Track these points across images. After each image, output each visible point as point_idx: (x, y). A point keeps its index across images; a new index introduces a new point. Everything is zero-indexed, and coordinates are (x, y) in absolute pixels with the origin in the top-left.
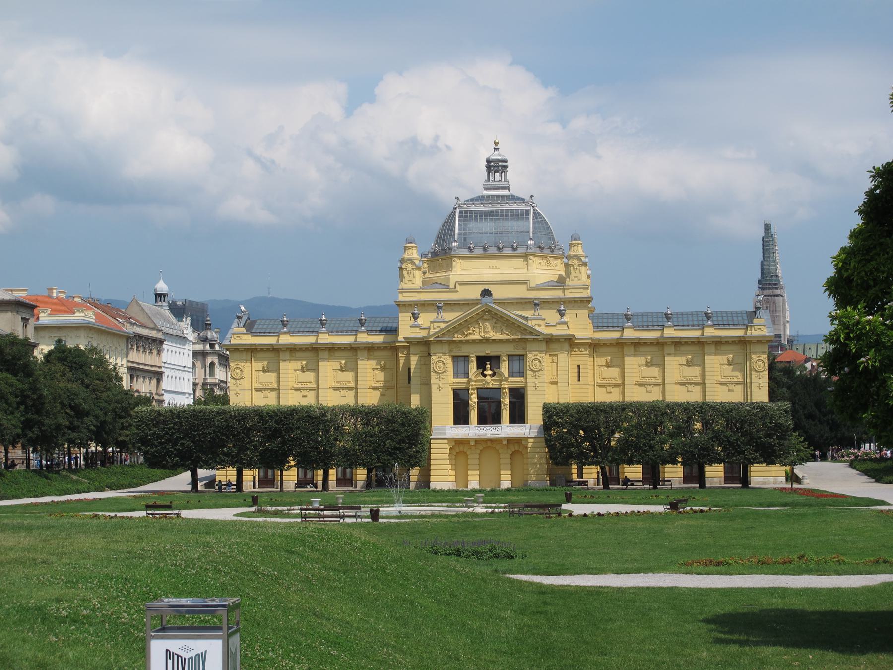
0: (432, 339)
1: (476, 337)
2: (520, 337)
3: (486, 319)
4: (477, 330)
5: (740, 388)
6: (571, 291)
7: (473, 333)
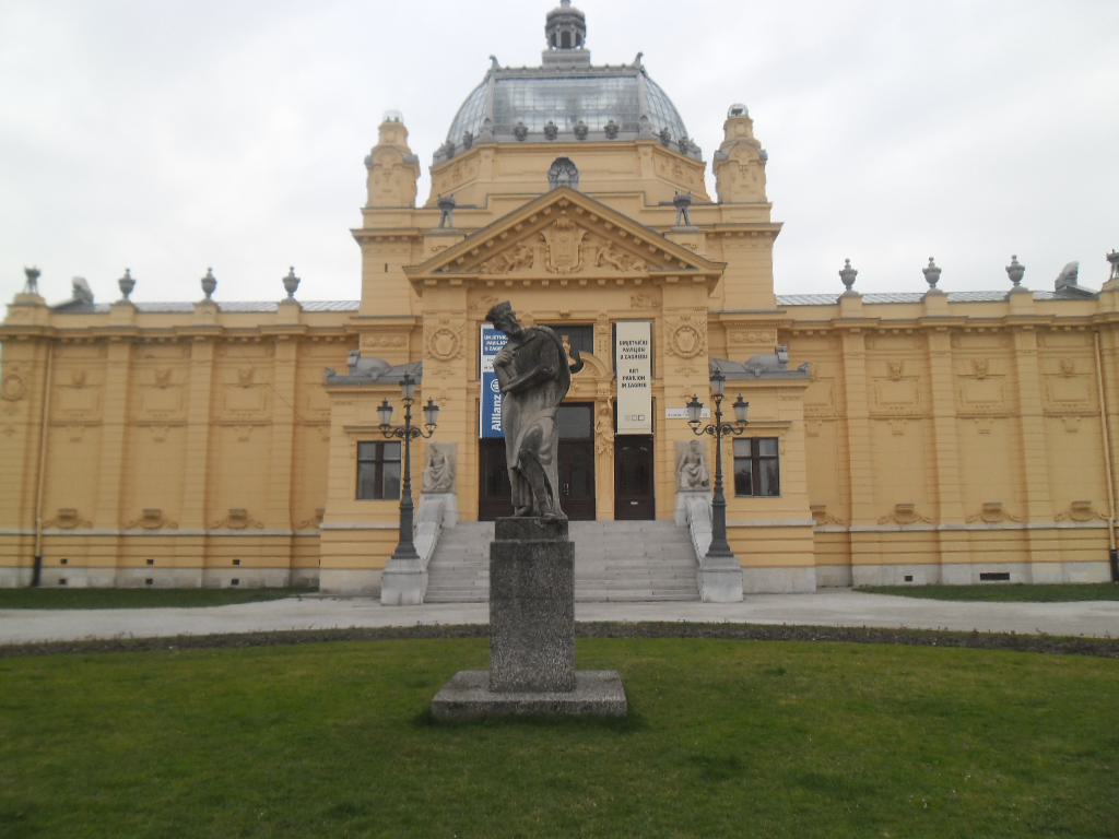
0: (426, 274)
1: (537, 272)
2: (644, 274)
3: (561, 228)
4: (537, 255)
5: (1088, 426)
6: (735, 214)
7: (528, 262)
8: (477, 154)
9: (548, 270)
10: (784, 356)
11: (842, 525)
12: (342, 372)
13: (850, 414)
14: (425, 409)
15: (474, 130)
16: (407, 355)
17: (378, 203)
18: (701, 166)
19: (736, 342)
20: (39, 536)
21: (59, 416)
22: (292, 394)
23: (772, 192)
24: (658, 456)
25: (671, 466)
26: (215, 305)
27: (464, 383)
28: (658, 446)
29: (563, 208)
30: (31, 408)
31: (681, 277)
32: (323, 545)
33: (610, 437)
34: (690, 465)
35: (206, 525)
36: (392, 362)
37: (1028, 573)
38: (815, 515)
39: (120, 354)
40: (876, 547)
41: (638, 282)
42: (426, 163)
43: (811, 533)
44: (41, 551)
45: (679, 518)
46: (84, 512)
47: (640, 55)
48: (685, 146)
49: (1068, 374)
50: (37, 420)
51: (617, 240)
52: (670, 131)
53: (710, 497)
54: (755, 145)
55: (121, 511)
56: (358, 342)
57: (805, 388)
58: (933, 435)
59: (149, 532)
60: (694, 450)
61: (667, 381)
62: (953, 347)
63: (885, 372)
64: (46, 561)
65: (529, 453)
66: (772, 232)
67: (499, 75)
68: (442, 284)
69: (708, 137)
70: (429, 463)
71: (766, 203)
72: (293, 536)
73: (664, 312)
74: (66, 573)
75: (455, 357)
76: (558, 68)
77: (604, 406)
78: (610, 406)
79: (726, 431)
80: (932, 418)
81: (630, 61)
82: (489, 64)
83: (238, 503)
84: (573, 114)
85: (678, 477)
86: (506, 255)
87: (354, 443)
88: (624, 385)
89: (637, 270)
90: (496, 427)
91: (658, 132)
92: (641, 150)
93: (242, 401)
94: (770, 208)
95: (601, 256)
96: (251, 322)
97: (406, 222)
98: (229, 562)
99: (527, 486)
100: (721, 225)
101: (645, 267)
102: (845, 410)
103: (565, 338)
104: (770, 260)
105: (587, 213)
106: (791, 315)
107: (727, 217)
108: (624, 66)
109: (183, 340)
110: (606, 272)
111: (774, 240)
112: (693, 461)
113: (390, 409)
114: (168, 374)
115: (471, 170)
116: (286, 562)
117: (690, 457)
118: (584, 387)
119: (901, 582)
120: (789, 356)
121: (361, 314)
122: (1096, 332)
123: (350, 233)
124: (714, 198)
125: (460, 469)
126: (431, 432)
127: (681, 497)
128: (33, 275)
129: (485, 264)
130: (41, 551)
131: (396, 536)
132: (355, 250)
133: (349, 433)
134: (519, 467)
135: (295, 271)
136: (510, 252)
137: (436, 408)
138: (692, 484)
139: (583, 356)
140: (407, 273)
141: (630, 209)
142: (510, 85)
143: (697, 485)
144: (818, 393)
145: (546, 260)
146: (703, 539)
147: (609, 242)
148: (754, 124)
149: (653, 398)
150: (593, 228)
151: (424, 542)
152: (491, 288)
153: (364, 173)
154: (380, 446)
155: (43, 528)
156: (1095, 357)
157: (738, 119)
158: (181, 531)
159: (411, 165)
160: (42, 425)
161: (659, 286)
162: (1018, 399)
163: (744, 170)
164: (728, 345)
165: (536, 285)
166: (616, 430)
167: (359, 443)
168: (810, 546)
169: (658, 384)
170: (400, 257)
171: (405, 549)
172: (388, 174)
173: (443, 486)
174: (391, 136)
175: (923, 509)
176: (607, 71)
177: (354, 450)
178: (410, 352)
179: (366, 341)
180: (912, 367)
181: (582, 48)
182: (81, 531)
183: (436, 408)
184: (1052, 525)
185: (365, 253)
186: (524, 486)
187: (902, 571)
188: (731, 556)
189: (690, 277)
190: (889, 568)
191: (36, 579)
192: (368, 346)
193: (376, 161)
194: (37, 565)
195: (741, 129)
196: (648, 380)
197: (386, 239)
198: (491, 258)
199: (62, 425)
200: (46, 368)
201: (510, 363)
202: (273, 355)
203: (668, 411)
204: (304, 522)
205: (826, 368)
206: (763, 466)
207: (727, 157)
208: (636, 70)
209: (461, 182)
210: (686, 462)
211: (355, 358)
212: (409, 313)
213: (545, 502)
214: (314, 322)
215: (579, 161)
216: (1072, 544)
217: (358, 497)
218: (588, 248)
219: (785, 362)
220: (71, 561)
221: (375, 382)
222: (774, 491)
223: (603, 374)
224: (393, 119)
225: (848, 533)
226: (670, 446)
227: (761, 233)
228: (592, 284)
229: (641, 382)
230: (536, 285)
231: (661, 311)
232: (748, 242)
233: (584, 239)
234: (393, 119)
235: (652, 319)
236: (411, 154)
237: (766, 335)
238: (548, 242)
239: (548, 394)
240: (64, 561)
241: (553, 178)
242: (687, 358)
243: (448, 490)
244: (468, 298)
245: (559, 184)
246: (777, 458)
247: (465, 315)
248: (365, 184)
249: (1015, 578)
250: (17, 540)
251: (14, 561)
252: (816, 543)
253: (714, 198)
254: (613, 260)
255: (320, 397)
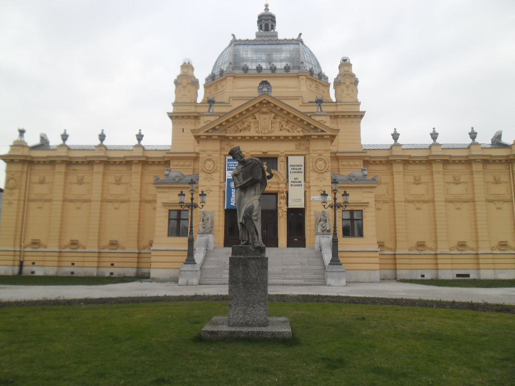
0: (201, 133)
1: (252, 133)
2: (301, 134)
4: (252, 125)
6: (344, 107)
8: (225, 78)
9: (257, 132)
10: (366, 172)
11: (392, 251)
12: (162, 178)
13: (396, 199)
14: (200, 195)
15: (224, 68)
16: (192, 170)
17: (180, 101)
18: (328, 85)
19: (343, 166)
20: (22, 252)
21: (32, 197)
22: (139, 188)
23: (360, 98)
24: (307, 218)
25: (313, 223)
26: (105, 147)
27: (218, 184)
28: (307, 213)
29: (265, 104)
30: (20, 193)
31: (318, 136)
32: (152, 257)
33: (285, 209)
34: (322, 223)
35: (99, 247)
36: (185, 174)
37: (479, 274)
38: (380, 246)
39: (61, 168)
40: (408, 261)
41: (299, 138)
42: (202, 82)
43: (377, 254)
44: (23, 258)
45: (317, 247)
46: (43, 240)
47: (300, 34)
48: (321, 76)
49: (497, 182)
50: (22, 198)
51: (289, 119)
52: (314, 69)
53: (331, 237)
54: (353, 76)
55: (60, 240)
56: (170, 164)
57: (376, 187)
58: (434, 210)
59: (72, 250)
60: (324, 215)
61: (311, 184)
62: (444, 169)
63: (412, 180)
64: (25, 263)
65: (248, 216)
66: (360, 115)
67: (235, 43)
68: (209, 138)
69: (331, 72)
70: (202, 220)
71: (358, 102)
72: (139, 253)
73: (311, 152)
74: (34, 269)
75: (214, 172)
76: (263, 40)
77: (282, 195)
78: (285, 195)
79: (339, 207)
80: (433, 201)
81: (296, 37)
82: (232, 38)
83: (114, 238)
84: (270, 61)
85: (316, 228)
86: (238, 125)
87: (167, 210)
88: (292, 185)
89: (298, 132)
90: (233, 204)
91: (308, 69)
92: (301, 77)
93: (116, 190)
94: (360, 105)
95: (282, 126)
96: (122, 155)
97: (192, 109)
98: (109, 264)
99: (246, 231)
100: (338, 112)
101: (302, 131)
102: (394, 198)
103: (265, 163)
104: (359, 128)
105: (275, 106)
106: (369, 154)
107: (340, 109)
108: (293, 39)
109: (90, 163)
110: (284, 133)
111: (361, 119)
112: (323, 221)
113: (184, 195)
114: (83, 178)
115: (223, 86)
116: (135, 265)
117: (322, 218)
118: (273, 186)
119: (419, 278)
120: (368, 173)
121: (171, 151)
122: (510, 163)
123: (167, 115)
124: (334, 100)
125: (216, 223)
126: (203, 206)
127: (317, 237)
128: (22, 132)
129: (229, 129)
130: (23, 258)
131: (186, 253)
132: (169, 122)
133: (165, 206)
134: (243, 222)
135: (141, 131)
136: (240, 124)
137: (205, 195)
138: (323, 231)
139: (273, 171)
140: (192, 133)
141: (295, 104)
142: (241, 47)
143: (325, 232)
144: (381, 190)
145: (256, 128)
146: (328, 257)
147: (286, 119)
148: (352, 66)
149: (305, 191)
150: (277, 112)
151: (199, 257)
152: (231, 140)
153: (174, 87)
154: (179, 212)
155: (24, 248)
156: (510, 175)
157: (345, 64)
158: (87, 250)
159: (195, 83)
160: (25, 201)
161: (308, 140)
162: (474, 193)
163: (348, 87)
164: (340, 167)
165: (252, 139)
166: (287, 205)
167: (170, 210)
168: (377, 260)
169: (307, 185)
170: (189, 126)
171: (190, 260)
172: (185, 87)
173: (208, 231)
174: (186, 70)
175: (429, 244)
176: (285, 41)
177: (167, 214)
178: (194, 169)
179: (173, 163)
180: (425, 178)
181: (274, 31)
182: (42, 249)
183: (205, 195)
184: (489, 252)
185: (173, 123)
186: (245, 231)
187: (420, 273)
188: (341, 264)
189: (323, 136)
190: (414, 271)
191: (20, 272)
192: (175, 166)
193: (179, 82)
194: (21, 265)
195: (346, 68)
196: (303, 183)
197: (183, 117)
198: (231, 126)
199: (34, 201)
200: (27, 174)
201: (239, 174)
202: (131, 170)
203: (312, 197)
204: (144, 247)
205: (384, 178)
206: (356, 223)
207: (340, 81)
208: (299, 41)
209: (218, 92)
210: (320, 221)
211: (168, 171)
212: (193, 151)
213: (255, 239)
214: (149, 155)
215: (272, 82)
216: (498, 261)
217: (168, 236)
218: (276, 122)
219: (366, 175)
220: (37, 263)
221: (177, 183)
222: (361, 234)
223: (282, 180)
224: (187, 63)
225: (395, 254)
226: (312, 213)
227: (355, 116)
228: (278, 138)
229: (299, 184)
230: (252, 139)
231: (309, 151)
232: (349, 120)
233: (274, 118)
234: (187, 63)
235: (305, 155)
236: (195, 78)
237: (357, 163)
238: (257, 119)
239: (257, 188)
240: (33, 263)
241: (260, 90)
242: (320, 173)
243: (210, 232)
244: (220, 144)
245: (263, 93)
246: (362, 219)
247: (219, 152)
248: (174, 92)
249: (472, 277)
250: (12, 253)
251: (11, 263)
252: (380, 259)
253: (334, 100)
254: (287, 128)
255: (152, 189)
